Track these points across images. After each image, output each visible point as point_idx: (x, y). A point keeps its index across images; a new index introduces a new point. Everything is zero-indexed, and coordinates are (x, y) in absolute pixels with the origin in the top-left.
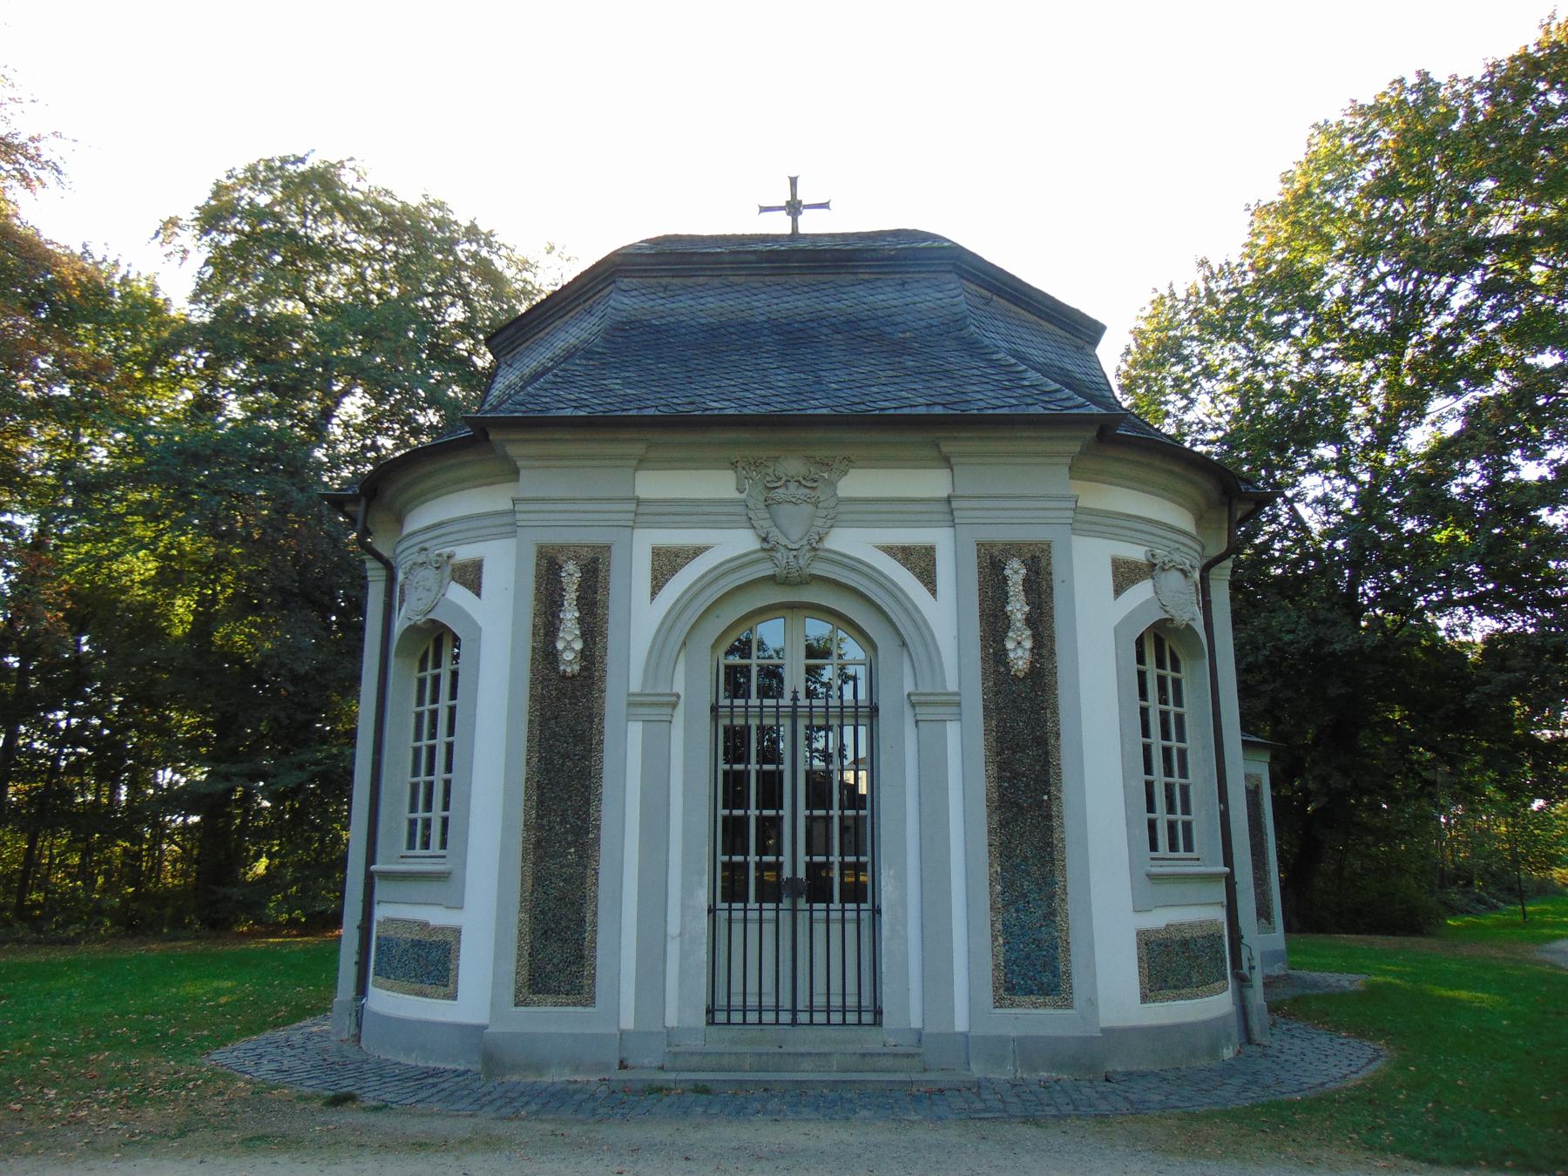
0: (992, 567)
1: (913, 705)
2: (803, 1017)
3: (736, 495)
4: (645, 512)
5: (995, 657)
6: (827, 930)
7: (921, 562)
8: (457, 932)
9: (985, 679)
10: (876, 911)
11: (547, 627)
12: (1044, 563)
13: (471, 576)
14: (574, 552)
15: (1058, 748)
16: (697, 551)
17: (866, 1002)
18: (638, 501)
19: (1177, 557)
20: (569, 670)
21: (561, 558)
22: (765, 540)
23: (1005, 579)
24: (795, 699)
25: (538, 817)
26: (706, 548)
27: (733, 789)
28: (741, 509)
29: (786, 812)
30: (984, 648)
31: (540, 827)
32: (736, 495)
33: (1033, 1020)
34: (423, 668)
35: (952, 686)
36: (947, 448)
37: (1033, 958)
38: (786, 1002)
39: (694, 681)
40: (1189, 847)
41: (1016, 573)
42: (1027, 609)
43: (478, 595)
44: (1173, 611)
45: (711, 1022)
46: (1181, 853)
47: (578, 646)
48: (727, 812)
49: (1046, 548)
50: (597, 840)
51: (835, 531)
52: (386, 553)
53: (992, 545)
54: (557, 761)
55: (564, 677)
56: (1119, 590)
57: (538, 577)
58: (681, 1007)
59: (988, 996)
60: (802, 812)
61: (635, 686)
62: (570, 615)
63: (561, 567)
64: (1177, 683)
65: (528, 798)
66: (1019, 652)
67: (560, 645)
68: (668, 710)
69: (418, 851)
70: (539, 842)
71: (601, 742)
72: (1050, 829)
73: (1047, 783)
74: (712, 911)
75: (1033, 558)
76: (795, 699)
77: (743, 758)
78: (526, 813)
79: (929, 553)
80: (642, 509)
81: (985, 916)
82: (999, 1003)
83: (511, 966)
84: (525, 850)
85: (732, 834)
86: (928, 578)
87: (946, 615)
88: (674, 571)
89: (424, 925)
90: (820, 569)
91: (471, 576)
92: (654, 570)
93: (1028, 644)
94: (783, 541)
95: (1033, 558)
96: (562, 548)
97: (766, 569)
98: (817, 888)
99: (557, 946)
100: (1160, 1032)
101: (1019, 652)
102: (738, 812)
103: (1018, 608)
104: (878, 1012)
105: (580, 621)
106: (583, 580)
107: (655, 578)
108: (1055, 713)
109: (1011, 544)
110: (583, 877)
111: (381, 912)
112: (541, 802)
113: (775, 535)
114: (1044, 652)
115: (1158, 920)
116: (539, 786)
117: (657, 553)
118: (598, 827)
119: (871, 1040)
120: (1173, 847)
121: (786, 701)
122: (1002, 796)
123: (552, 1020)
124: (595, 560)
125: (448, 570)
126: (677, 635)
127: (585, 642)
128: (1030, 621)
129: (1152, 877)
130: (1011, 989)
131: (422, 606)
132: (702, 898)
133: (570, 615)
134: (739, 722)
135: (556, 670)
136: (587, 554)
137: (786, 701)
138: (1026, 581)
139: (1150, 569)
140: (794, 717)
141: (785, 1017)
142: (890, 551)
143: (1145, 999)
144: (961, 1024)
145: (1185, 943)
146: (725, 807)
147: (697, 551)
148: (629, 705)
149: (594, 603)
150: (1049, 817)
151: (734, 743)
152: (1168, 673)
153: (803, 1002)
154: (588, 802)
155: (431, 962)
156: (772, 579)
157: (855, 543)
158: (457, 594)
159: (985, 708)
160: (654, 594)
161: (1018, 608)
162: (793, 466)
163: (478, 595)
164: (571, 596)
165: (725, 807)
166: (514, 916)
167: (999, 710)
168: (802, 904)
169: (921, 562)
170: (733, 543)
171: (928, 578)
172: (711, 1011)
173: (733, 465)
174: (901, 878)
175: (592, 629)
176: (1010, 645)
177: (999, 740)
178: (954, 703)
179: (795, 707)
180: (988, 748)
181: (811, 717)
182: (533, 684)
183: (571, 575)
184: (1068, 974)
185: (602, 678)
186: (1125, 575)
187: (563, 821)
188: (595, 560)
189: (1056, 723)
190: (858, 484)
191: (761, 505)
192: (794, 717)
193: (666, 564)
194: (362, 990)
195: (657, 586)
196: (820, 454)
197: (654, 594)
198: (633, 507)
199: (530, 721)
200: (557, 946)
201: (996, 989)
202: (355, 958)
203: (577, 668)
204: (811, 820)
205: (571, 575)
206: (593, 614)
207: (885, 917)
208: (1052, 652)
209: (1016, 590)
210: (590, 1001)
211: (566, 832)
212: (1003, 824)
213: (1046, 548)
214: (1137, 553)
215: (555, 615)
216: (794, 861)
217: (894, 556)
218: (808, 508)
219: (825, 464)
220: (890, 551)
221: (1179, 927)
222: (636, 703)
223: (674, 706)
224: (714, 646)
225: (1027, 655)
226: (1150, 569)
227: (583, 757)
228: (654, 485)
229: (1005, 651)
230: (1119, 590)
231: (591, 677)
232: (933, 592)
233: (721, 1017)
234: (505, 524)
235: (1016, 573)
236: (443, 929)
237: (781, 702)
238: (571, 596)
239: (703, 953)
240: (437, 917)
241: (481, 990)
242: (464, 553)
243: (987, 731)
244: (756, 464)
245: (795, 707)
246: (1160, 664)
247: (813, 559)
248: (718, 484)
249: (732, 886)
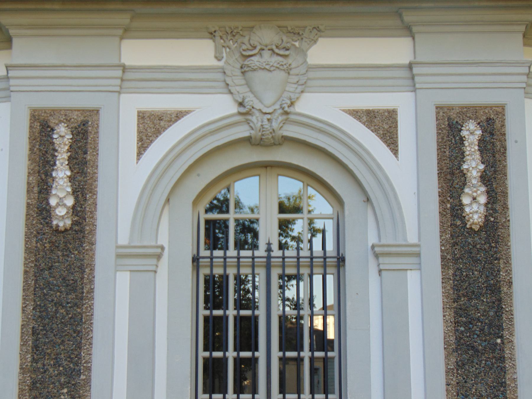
0: (450, 129)
1: (377, 256)
3: (215, 63)
4: (129, 77)
7: (384, 125)
9: (442, 232)
12: (498, 124)
14: (65, 115)
15: (510, 296)
16: (179, 115)
18: (124, 68)
20: (61, 224)
21: (52, 122)
22: (241, 104)
23: (462, 140)
24: (269, 250)
25: (34, 361)
26: (187, 112)
27: (213, 333)
28: (220, 76)
29: (261, 354)
30: (442, 203)
31: (35, 370)
32: (215, 63)
35: (412, 238)
36: (409, 17)
39: (177, 234)
41: (472, 134)
42: (482, 167)
47: (70, 202)
48: (207, 354)
49: (499, 111)
50: (88, 381)
51: (306, 96)
53: (450, 108)
54: (51, 308)
55: (57, 231)
57: (32, 139)
60: (276, 354)
61: (123, 239)
62: (62, 173)
63: (53, 130)
65: (24, 344)
67: (53, 202)
68: (154, 261)
70: (34, 383)
71: (91, 291)
72: (503, 370)
73: (500, 328)
75: (489, 120)
76: (269, 250)
77: (221, 304)
78: (22, 357)
80: (129, 75)
84: (21, 390)
86: (390, 139)
87: (407, 174)
88: (158, 132)
90: (291, 131)
92: (139, 132)
93: (483, 199)
94: (258, 106)
95: (489, 120)
96: (54, 112)
97: (243, 132)
102: (218, 354)
103: (473, 166)
105: (71, 179)
106: (74, 141)
107: (140, 140)
108: (508, 262)
109: (468, 108)
112: (36, 347)
113: (251, 100)
114: (498, 207)
116: (34, 332)
117: (142, 116)
118: (89, 369)
121: (261, 252)
122: (458, 339)
124: (85, 123)
126: (163, 192)
127: (76, 198)
128: (484, 178)
133: (62, 173)
134: (218, 271)
135: (49, 224)
136: (78, 118)
137: (261, 252)
138: (482, 142)
140: (268, 267)
142: (355, 114)
146: (205, 349)
147: (179, 115)
148: (119, 256)
150: (502, 359)
151: (214, 291)
154: (79, 347)
156: (248, 141)
157: (326, 108)
159: (443, 258)
160: (140, 154)
161: (473, 166)
162: (266, 35)
164: (62, 157)
165: (205, 349)
167: (456, 260)
169: (384, 125)
170: (210, 109)
171: (390, 139)
173: (212, 35)
175: (83, 187)
176: (466, 200)
177: (456, 288)
178: (415, 254)
179: (269, 257)
180: (446, 294)
181: (283, 266)
183: (63, 137)
185: (93, 232)
187: (57, 364)
188: (85, 123)
189: (509, 272)
190: (327, 51)
191: (238, 72)
192: (268, 267)
193: (151, 126)
195: (143, 146)
196: (291, 24)
197: (140, 154)
198: (119, 73)
199: (26, 272)
203: (69, 222)
204: (283, 361)
205: (63, 137)
206: (82, 173)
208: (505, 207)
211: (59, 374)
212: (460, 365)
213: (499, 111)
217: (359, 119)
218: (281, 75)
219: (296, 34)
220: (355, 114)
222: (123, 255)
223: (159, 257)
224: (196, 202)
225: (482, 209)
227: (76, 305)
228: (139, 52)
229: (461, 206)
231: (82, 231)
232: (395, 151)
235: (472, 134)
237: (257, 253)
238: (62, 157)
244: (233, 34)
245: (269, 257)
247: (286, 121)
248: (196, 52)
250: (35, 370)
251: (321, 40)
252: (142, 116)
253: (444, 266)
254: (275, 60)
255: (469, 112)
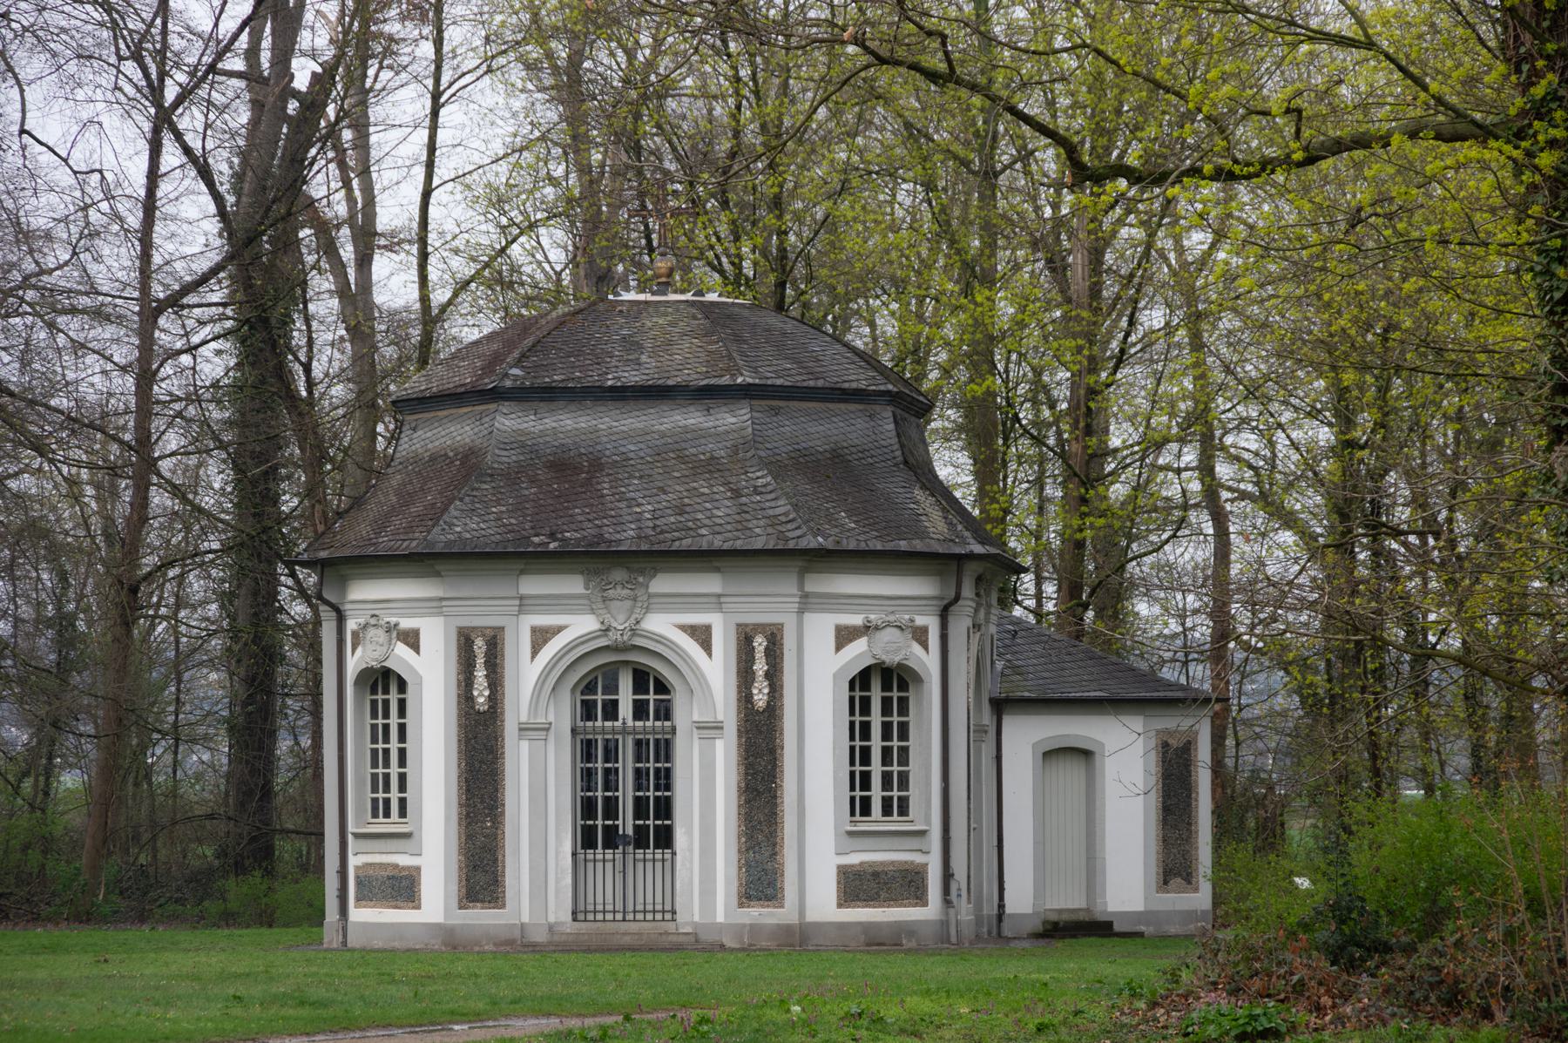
2: (630, 917)
4: (525, 604)
5: (745, 698)
6: (645, 866)
7: (702, 636)
8: (418, 869)
9: (739, 712)
10: (674, 854)
11: (466, 682)
13: (412, 639)
14: (481, 630)
17: (668, 907)
18: (521, 598)
19: (891, 618)
21: (473, 636)
30: (739, 692)
33: (758, 914)
34: (374, 691)
37: (761, 877)
38: (619, 906)
39: (562, 714)
40: (904, 810)
41: (760, 643)
43: (418, 653)
44: (884, 657)
45: (575, 920)
46: (895, 817)
47: (487, 693)
50: (503, 813)
51: (650, 616)
52: (333, 599)
53: (747, 625)
54: (477, 765)
56: (838, 648)
57: (459, 648)
58: (559, 910)
59: (735, 901)
61: (524, 718)
62: (480, 673)
64: (903, 702)
65: (460, 788)
66: (760, 697)
67: (475, 693)
69: (381, 819)
72: (776, 805)
74: (574, 854)
78: (460, 797)
79: (707, 629)
80: (525, 602)
81: (734, 856)
82: (741, 905)
83: (454, 887)
85: (588, 808)
86: (706, 646)
88: (546, 641)
89: (397, 866)
91: (412, 639)
93: (766, 691)
94: (615, 624)
96: (474, 628)
98: (640, 840)
99: (481, 874)
100: (842, 926)
101: (760, 697)
103: (760, 667)
104: (674, 912)
106: (488, 650)
110: (495, 837)
111: (354, 861)
112: (468, 790)
115: (854, 859)
117: (534, 630)
119: (671, 927)
120: (887, 810)
123: (481, 917)
124: (495, 637)
125: (394, 634)
126: (551, 683)
128: (768, 675)
129: (850, 834)
130: (749, 898)
131: (376, 655)
132: (567, 847)
133: (480, 673)
139: (867, 629)
141: (619, 916)
142: (683, 628)
143: (840, 906)
144: (720, 918)
145: (876, 875)
148: (521, 729)
149: (495, 665)
150: (775, 797)
151: (587, 750)
152: (895, 694)
153: (630, 907)
155: (403, 887)
156: (607, 647)
157: (662, 625)
158: (401, 650)
160: (533, 657)
161: (760, 667)
162: (619, 575)
163: (418, 653)
164: (480, 661)
166: (455, 857)
168: (630, 849)
170: (581, 625)
171: (706, 646)
172: (574, 913)
173: (582, 573)
174: (690, 833)
175: (495, 682)
176: (755, 691)
177: (747, 751)
178: (718, 727)
180: (740, 755)
182: (459, 716)
183: (480, 645)
184: (782, 889)
185: (502, 713)
186: (844, 636)
188: (495, 637)
190: (663, 584)
193: (541, 637)
194: (343, 911)
195: (535, 652)
197: (533, 657)
200: (481, 874)
201: (740, 898)
202: (336, 893)
205: (480, 645)
206: (495, 672)
207: (679, 858)
209: (761, 655)
210: (503, 906)
212: (748, 801)
214: (857, 620)
215: (471, 673)
216: (627, 823)
218: (629, 603)
219: (642, 572)
220: (683, 628)
221: (872, 864)
222: (523, 729)
223: (547, 730)
226: (867, 629)
228: (532, 585)
229: (751, 695)
230: (838, 648)
233: (581, 916)
234: (436, 606)
235: (760, 643)
236: (408, 868)
238: (480, 661)
239: (569, 880)
240: (404, 860)
241: (437, 901)
242: (406, 623)
243: (740, 745)
244: (597, 573)
246: (886, 687)
248: (573, 585)
249: (587, 839)
250: (468, 806)
251: (659, 575)
252: (534, 630)
253: (739, 737)
254: (626, 592)
255: (759, 628)
